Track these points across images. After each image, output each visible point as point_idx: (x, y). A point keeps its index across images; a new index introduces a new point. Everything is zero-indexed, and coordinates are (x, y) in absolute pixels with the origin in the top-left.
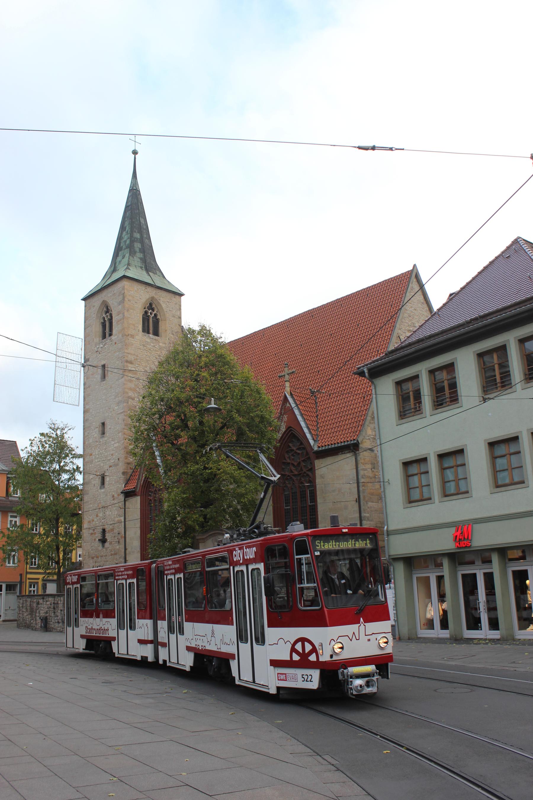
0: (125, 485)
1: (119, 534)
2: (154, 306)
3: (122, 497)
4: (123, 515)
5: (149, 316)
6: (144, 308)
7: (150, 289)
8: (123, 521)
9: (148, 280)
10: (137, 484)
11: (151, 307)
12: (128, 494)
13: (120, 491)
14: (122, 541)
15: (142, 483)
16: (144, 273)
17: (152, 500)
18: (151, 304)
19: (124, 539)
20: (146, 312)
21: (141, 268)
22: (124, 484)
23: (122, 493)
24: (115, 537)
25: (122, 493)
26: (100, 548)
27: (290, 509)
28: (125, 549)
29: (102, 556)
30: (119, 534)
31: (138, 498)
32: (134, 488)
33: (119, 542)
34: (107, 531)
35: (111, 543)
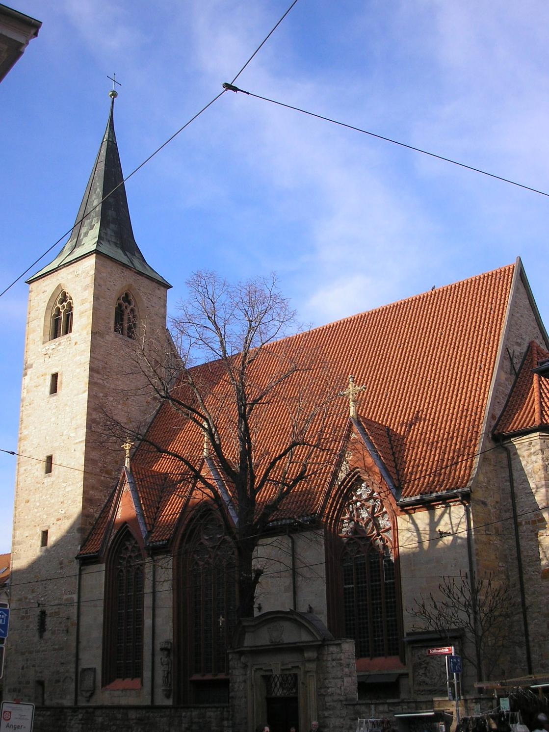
0: (81, 548)
1: (68, 619)
2: (131, 297)
3: (76, 565)
4: (77, 590)
5: (122, 311)
6: (118, 299)
7: (127, 273)
8: (76, 600)
9: (124, 260)
10: (102, 547)
11: (127, 298)
12: (85, 561)
13: (72, 556)
14: (73, 630)
15: (109, 545)
16: (120, 251)
17: (124, 571)
18: (127, 295)
19: (76, 627)
20: (120, 305)
21: (116, 244)
22: (79, 546)
23: (76, 558)
24: (61, 623)
25: (76, 558)
26: (36, 639)
27: (353, 588)
28: (78, 642)
29: (38, 652)
30: (68, 619)
31: (103, 567)
32: (97, 552)
33: (67, 631)
34: (49, 615)
35: (53, 633)
